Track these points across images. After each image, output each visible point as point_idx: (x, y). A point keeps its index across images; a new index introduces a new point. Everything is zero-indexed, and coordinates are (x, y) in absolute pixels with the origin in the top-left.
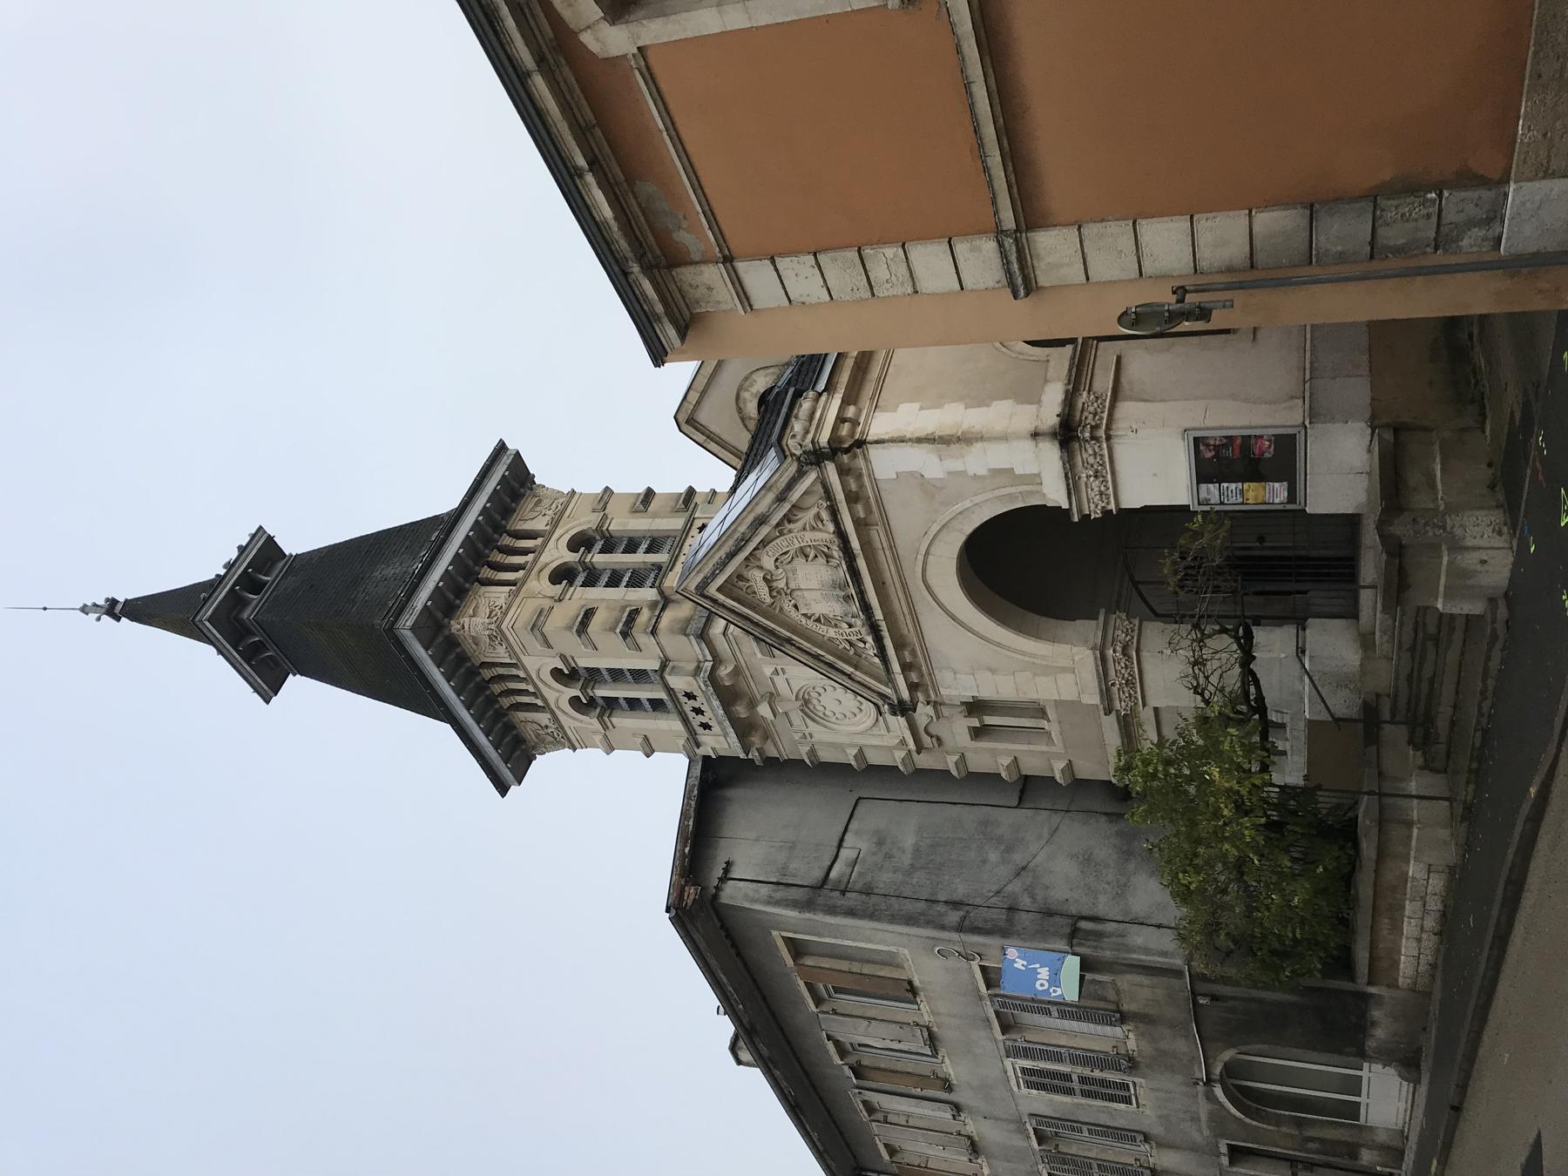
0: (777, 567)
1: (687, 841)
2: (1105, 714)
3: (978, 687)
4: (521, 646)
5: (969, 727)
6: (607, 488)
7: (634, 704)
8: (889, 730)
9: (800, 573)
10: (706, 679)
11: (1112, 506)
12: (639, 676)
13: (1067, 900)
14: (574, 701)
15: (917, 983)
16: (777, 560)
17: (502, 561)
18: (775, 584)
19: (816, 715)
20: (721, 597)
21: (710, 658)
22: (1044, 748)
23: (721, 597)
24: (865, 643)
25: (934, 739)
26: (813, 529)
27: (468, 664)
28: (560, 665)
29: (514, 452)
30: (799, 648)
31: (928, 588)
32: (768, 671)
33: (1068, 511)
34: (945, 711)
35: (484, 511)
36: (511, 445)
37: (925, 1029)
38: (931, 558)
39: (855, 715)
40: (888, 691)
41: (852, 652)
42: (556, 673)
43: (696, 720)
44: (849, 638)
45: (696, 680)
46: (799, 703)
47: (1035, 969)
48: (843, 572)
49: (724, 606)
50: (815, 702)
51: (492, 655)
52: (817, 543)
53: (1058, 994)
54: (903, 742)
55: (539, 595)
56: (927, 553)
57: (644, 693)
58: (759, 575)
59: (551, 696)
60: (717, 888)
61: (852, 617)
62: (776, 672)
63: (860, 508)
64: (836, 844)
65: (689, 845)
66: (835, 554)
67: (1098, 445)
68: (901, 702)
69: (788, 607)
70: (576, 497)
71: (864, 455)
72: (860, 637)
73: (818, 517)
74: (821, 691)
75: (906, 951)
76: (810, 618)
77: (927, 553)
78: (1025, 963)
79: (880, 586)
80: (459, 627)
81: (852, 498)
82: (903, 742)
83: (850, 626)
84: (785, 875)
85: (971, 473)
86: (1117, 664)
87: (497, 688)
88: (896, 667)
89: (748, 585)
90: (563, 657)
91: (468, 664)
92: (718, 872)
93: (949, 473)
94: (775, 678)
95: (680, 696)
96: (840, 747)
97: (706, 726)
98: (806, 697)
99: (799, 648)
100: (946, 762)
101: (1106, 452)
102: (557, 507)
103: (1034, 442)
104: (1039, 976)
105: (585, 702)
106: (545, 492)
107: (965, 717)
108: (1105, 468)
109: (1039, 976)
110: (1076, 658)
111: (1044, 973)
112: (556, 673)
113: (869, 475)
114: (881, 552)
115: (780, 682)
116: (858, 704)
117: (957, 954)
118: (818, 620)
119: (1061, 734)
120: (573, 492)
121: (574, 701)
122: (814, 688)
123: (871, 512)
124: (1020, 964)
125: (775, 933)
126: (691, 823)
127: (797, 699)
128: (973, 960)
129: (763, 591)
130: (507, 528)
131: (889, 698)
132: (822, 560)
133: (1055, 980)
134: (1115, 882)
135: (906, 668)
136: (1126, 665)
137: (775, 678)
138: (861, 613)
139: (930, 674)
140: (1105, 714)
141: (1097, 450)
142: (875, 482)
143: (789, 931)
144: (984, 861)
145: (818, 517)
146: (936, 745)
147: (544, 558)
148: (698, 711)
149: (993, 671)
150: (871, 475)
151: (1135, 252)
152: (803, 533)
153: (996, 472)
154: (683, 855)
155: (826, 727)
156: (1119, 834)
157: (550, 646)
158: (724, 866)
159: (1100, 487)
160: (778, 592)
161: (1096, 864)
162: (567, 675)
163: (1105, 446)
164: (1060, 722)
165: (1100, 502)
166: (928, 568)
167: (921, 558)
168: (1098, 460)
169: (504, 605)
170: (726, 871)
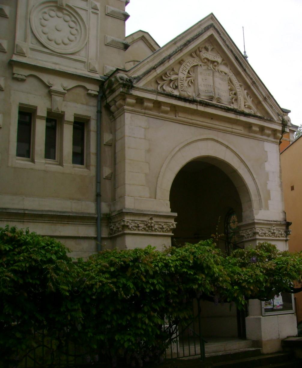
0: (221, 72)
3: (135, 138)
19: (49, 6)
25: (24, 78)
31: (207, 139)
32: (98, 5)
34: (58, 99)
38: (224, 148)
40: (141, 84)
41: (164, 78)
46: (64, 5)
48: (225, 102)
50: (60, 14)
54: (22, 54)
56: (227, 147)
58: (219, 60)
63: (257, 129)
68: (132, 87)
71: (276, 142)
73: (249, 108)
76: (190, 69)
77: (227, 147)
79: (213, 117)
81: (262, 129)
82: (22, 54)
88: (161, 99)
89: (210, 50)
98: (65, 12)
107: (48, 109)
113: (267, 140)
114: (231, 127)
116: (58, 42)
119: (32, 169)
123: (252, 132)
127: (67, 6)
131: (137, 82)
135: (158, 105)
138: (201, 99)
139: (145, 113)
142: (264, 140)
146: (15, 76)
149: (149, 151)
150: (267, 141)
160: (205, 63)
164: (45, 171)
166: (218, 145)
167: (226, 143)
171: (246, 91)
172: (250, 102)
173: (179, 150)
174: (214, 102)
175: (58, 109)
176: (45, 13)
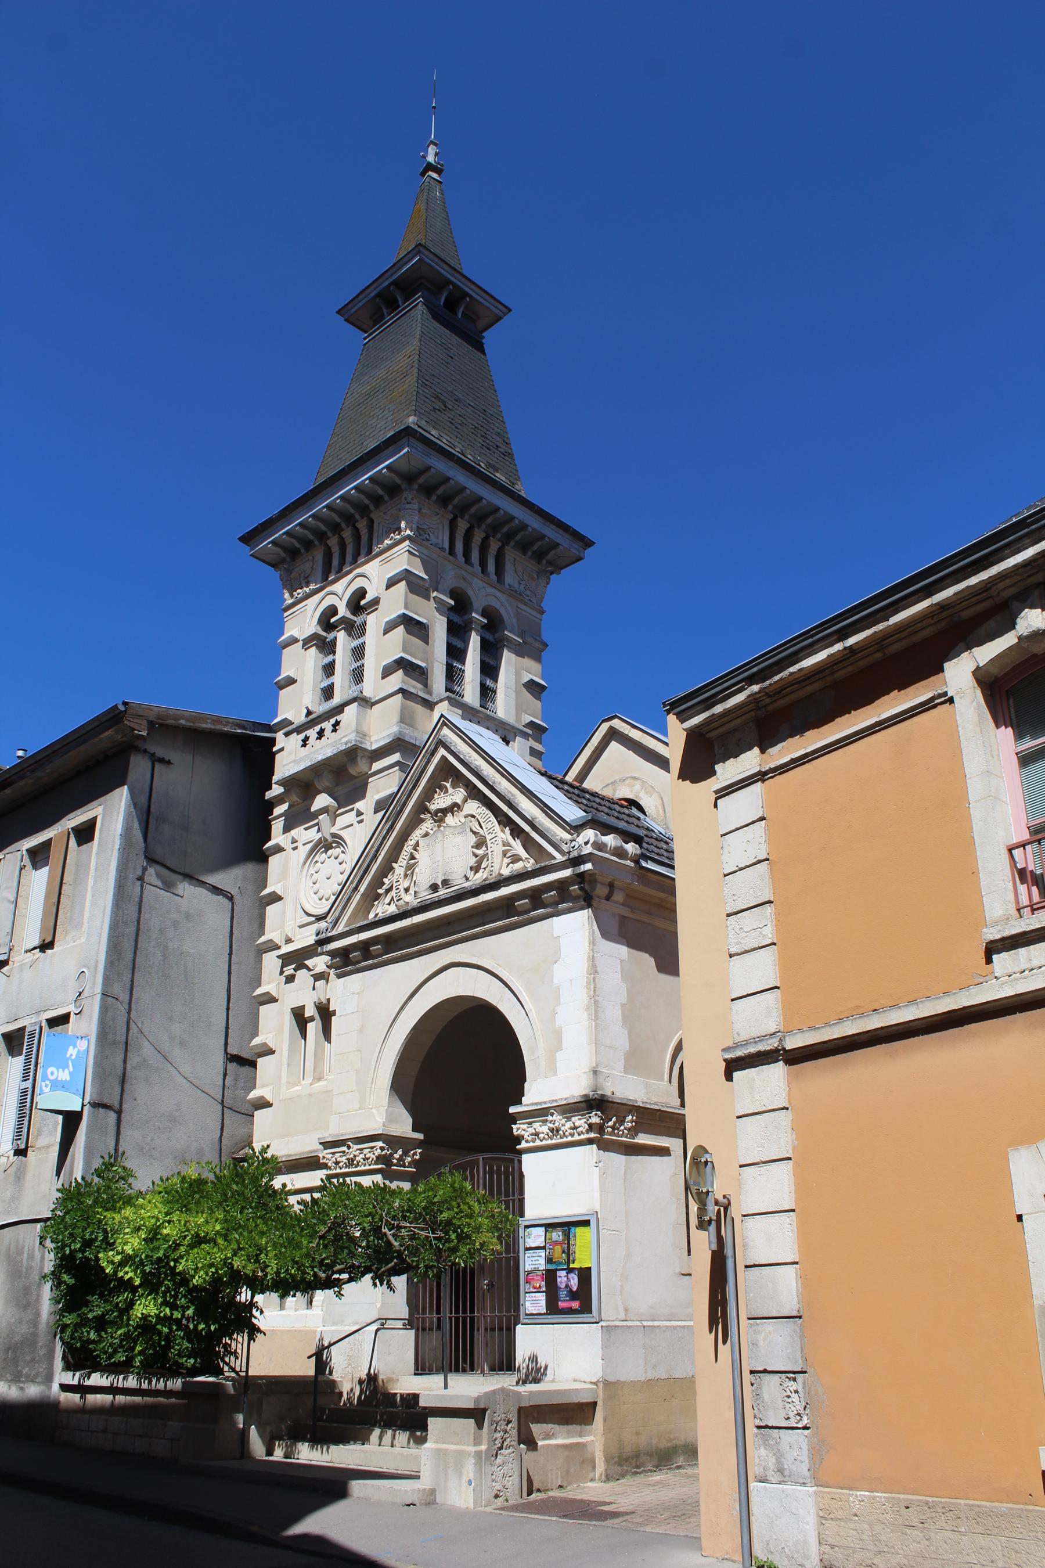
1: (193, 722)
2: (319, 1139)
3: (346, 1015)
4: (388, 559)
5: (304, 1006)
6: (547, 646)
7: (329, 669)
8: (301, 927)
9: (459, 839)
10: (353, 743)
11: (524, 1145)
12: (358, 675)
13: (135, 1100)
14: (332, 610)
15: (49, 952)
16: (473, 816)
17: (474, 541)
18: (449, 815)
20: (436, 760)
21: (374, 747)
22: (284, 1079)
23: (436, 760)
24: (389, 904)
26: (504, 854)
27: (372, 507)
28: (369, 597)
29: (582, 555)
30: (384, 838)
33: (520, 1103)
35: (524, 526)
36: (589, 551)
37: (6, 958)
39: (315, 893)
42: (361, 593)
43: (312, 733)
44: (394, 888)
45: (352, 732)
47: (68, 1067)
48: (459, 884)
49: (428, 762)
51: (380, 531)
52: (490, 858)
53: (44, 1088)
55: (439, 577)
57: (340, 679)
59: (339, 587)
60: (145, 751)
61: (415, 892)
62: (359, 813)
64: (187, 871)
65: (189, 724)
66: (479, 875)
67: (584, 1131)
69: (428, 825)
70: (538, 615)
72: (395, 899)
73: (516, 859)
74: (340, 860)
75: (83, 940)
78: (73, 1057)
80: (409, 499)
83: (407, 890)
84: (157, 820)
85: (557, 1009)
86: (369, 1150)
87: (347, 534)
90: (376, 601)
91: (372, 507)
92: (160, 752)
93: (558, 990)
94: (354, 813)
95: (338, 718)
96: (284, 874)
97: (305, 742)
99: (384, 838)
100: (269, 983)
101: (576, 1138)
102: (528, 596)
103: (587, 1070)
104: (61, 1070)
105: (332, 620)
106: (543, 584)
108: (561, 1138)
109: (61, 1070)
110: (374, 1111)
111: (64, 1075)
112: (361, 593)
115: (351, 817)
116: (326, 896)
117: (81, 990)
118: (412, 857)
119: (298, 1096)
120: (542, 612)
121: (332, 610)
122: (343, 852)
124: (72, 1052)
125: (100, 809)
126: (208, 726)
127: (334, 835)
128: (76, 1007)
129: (440, 801)
130: (506, 547)
132: (473, 861)
133: (57, 1085)
134: (153, 1146)
136: (368, 1159)
137: (354, 813)
138: (419, 900)
140: (319, 1139)
141: (579, 1130)
143: (102, 824)
144: (171, 1019)
145: (516, 859)
147: (477, 583)
148: (321, 734)
149: (361, 1030)
151: (763, 1160)
152: (501, 843)
153: (557, 1035)
154: (177, 718)
155: (305, 863)
156: (200, 1152)
157: (388, 587)
158: (167, 759)
159: (543, 1133)
161: (170, 1128)
162: (359, 603)
163: (583, 1137)
164: (310, 1095)
165: (528, 1134)
168: (569, 1131)
169: (430, 542)
170: (162, 760)
171: (507, 830)
172: (518, 848)
173: (402, 1008)
174: (443, 892)
175: (319, 999)
176: (317, 862)
